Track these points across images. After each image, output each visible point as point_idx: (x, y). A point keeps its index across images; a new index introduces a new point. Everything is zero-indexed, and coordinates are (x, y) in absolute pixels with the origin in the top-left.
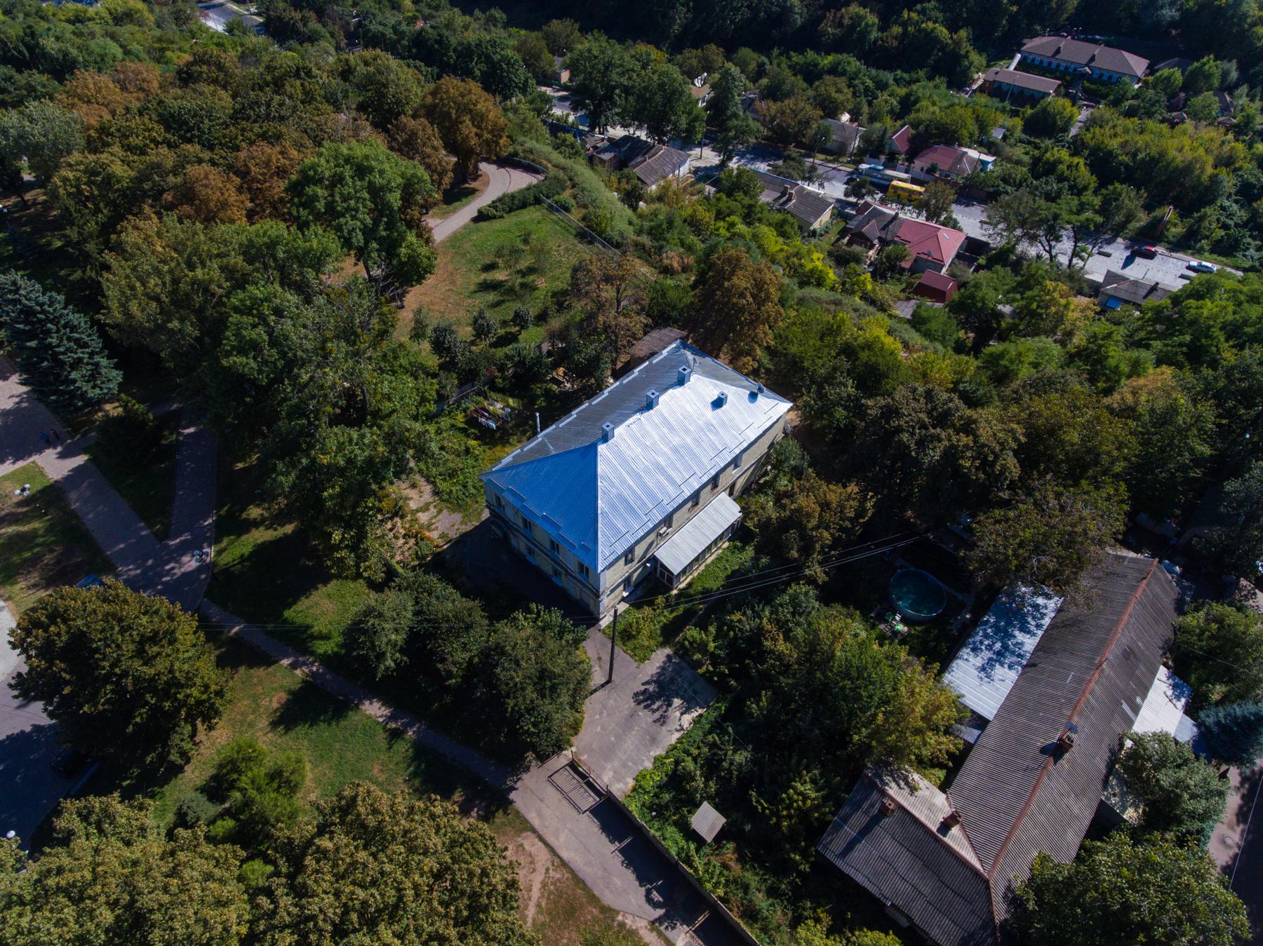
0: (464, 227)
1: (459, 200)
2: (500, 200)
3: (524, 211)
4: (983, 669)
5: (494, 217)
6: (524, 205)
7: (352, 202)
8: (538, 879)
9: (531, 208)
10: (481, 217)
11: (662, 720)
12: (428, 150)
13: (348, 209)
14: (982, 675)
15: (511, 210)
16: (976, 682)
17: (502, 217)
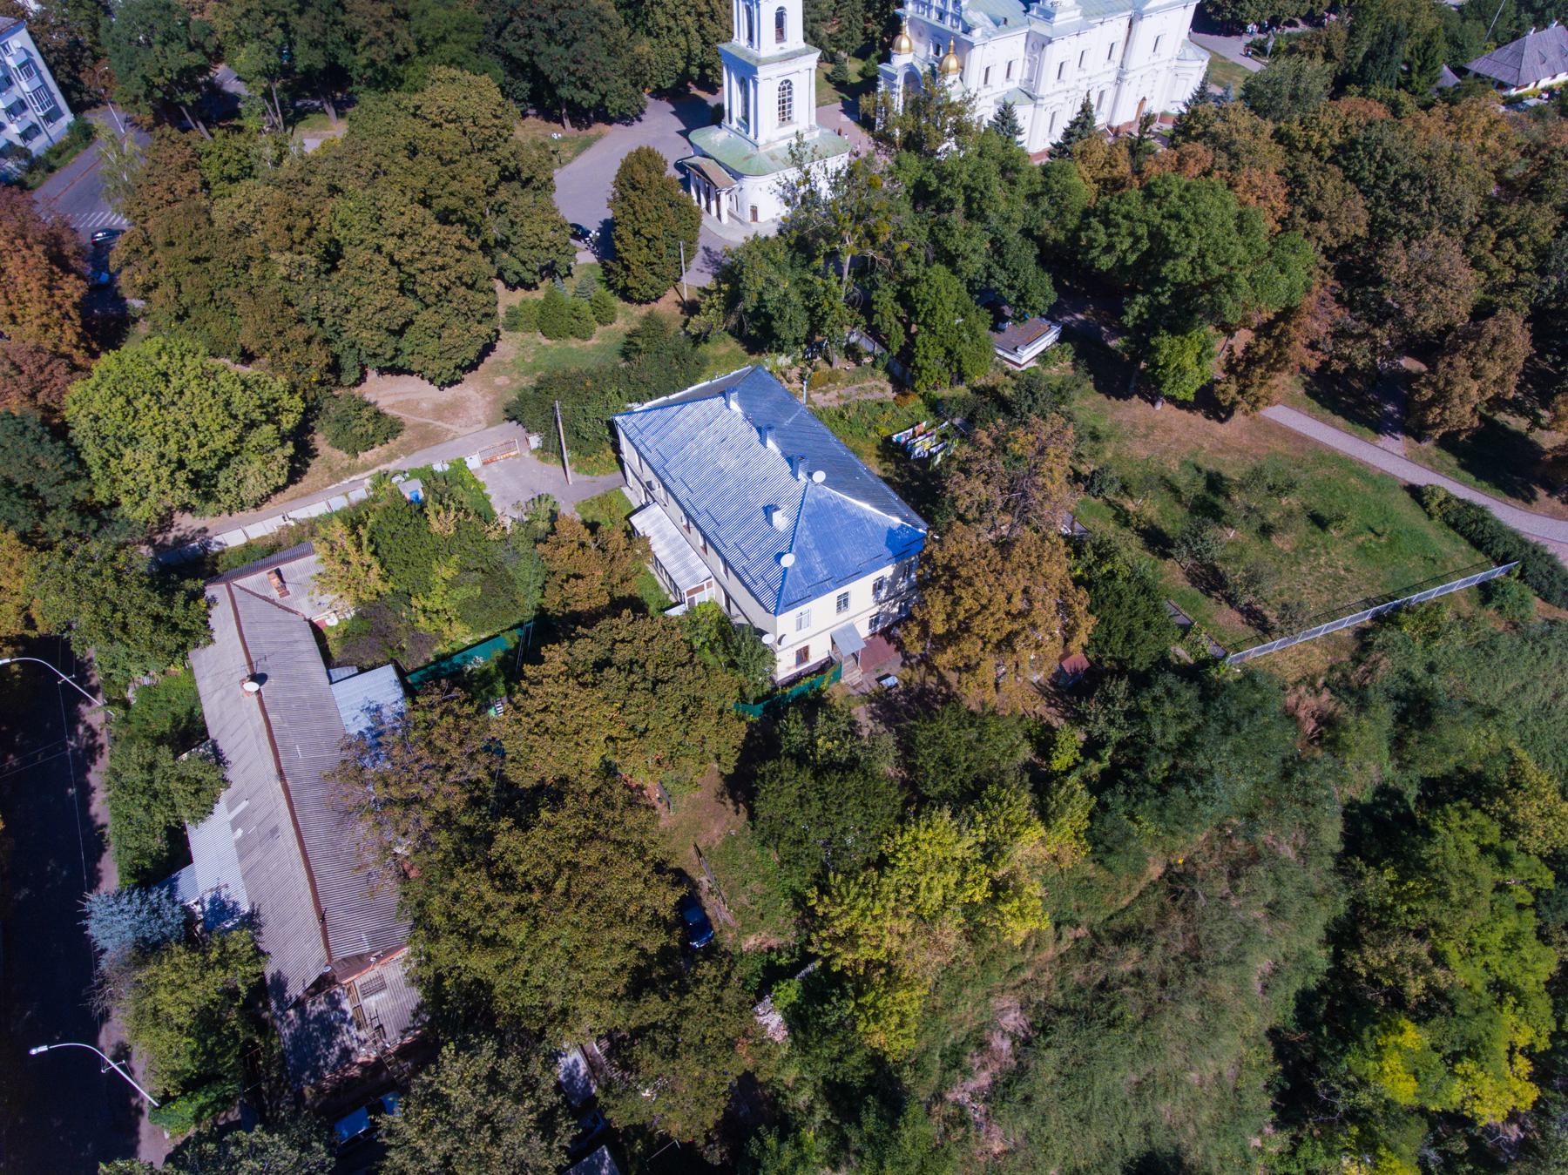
0: (1384, 475)
1: (1498, 486)
2: (1468, 505)
3: (1464, 546)
4: (378, 709)
5: (1424, 506)
6: (1477, 544)
7: (1125, 224)
8: (453, 428)
9: (1480, 557)
10: (1415, 492)
11: (517, 506)
12: (1461, 362)
13: (1118, 226)
14: (373, 706)
15: (1454, 526)
16: (371, 697)
17: (1430, 516)
